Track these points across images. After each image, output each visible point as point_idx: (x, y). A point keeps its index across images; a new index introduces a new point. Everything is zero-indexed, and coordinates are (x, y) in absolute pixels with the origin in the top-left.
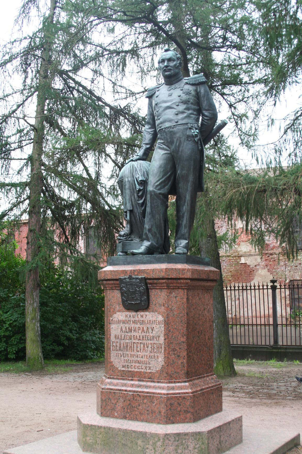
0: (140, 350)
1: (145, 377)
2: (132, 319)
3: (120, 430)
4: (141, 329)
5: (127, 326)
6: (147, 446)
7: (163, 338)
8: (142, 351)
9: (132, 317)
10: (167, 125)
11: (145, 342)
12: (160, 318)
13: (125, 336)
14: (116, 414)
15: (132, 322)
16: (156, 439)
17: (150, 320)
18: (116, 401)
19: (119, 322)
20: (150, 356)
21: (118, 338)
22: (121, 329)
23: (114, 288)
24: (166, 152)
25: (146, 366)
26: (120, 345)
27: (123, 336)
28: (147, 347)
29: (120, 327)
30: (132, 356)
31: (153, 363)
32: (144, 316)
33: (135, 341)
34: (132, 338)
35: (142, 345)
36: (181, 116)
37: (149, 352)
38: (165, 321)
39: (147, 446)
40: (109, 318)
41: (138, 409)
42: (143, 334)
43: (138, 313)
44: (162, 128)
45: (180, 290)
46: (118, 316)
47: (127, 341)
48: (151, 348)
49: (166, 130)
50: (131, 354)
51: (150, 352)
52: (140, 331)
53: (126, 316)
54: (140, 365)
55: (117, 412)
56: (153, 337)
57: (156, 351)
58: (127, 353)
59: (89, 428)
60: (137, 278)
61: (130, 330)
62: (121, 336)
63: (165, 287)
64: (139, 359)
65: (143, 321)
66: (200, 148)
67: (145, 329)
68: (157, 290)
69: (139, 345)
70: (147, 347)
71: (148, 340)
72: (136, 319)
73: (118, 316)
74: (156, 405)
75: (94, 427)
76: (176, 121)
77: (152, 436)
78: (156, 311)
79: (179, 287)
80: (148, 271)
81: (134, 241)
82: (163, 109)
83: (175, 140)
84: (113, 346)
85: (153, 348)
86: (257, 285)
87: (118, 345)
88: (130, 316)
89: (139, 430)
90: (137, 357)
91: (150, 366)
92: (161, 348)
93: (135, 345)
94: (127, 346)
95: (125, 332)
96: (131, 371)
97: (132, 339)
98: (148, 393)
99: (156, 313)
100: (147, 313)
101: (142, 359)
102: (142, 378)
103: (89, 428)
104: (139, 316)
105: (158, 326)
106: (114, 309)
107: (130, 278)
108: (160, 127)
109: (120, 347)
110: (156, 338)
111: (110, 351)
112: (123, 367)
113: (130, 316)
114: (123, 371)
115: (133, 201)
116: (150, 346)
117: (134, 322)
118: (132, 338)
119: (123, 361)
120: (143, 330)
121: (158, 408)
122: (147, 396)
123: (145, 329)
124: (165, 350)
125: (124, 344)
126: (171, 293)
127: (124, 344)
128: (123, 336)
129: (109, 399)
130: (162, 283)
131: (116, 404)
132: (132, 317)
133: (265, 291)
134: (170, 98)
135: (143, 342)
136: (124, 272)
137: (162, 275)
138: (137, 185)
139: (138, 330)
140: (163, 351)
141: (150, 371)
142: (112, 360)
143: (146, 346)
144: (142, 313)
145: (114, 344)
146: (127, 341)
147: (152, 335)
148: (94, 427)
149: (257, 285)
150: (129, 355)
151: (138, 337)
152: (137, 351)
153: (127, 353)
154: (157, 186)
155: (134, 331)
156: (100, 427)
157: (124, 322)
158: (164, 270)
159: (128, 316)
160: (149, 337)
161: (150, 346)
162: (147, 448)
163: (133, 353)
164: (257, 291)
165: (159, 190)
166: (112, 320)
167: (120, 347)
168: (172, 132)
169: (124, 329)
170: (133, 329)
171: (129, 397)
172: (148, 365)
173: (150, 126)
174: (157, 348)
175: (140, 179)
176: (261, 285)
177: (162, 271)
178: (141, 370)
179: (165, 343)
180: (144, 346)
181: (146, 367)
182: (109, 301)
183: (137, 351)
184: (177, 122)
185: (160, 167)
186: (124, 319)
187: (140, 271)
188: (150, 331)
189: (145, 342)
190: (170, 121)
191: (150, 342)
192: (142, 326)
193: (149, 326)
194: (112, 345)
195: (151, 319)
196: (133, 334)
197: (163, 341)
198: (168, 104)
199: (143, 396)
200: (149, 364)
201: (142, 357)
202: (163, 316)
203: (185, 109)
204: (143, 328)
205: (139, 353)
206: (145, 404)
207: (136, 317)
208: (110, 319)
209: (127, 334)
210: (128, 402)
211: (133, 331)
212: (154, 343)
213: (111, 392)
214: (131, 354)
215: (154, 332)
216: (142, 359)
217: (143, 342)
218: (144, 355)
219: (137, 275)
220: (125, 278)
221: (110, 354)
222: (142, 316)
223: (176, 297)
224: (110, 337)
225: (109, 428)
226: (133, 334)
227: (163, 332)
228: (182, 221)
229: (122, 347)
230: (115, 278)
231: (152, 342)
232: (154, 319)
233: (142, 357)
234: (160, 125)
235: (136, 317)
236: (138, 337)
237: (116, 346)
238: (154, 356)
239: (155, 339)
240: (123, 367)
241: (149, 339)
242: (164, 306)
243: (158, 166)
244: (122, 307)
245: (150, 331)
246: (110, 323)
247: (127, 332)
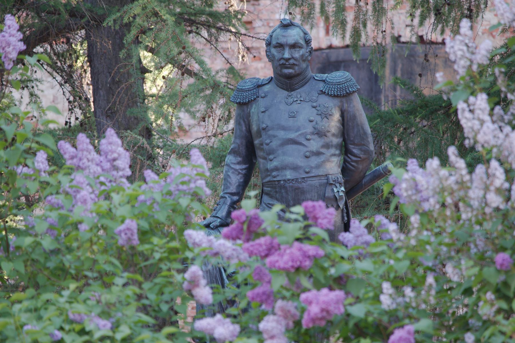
10: (289, 175)
44: (278, 178)
66: (346, 218)
76: (307, 170)
82: (279, 142)
168: (298, 188)
173: (239, 159)
184: (307, 173)
190: (295, 168)
198: (292, 135)
203: (323, 146)
234: (274, 173)
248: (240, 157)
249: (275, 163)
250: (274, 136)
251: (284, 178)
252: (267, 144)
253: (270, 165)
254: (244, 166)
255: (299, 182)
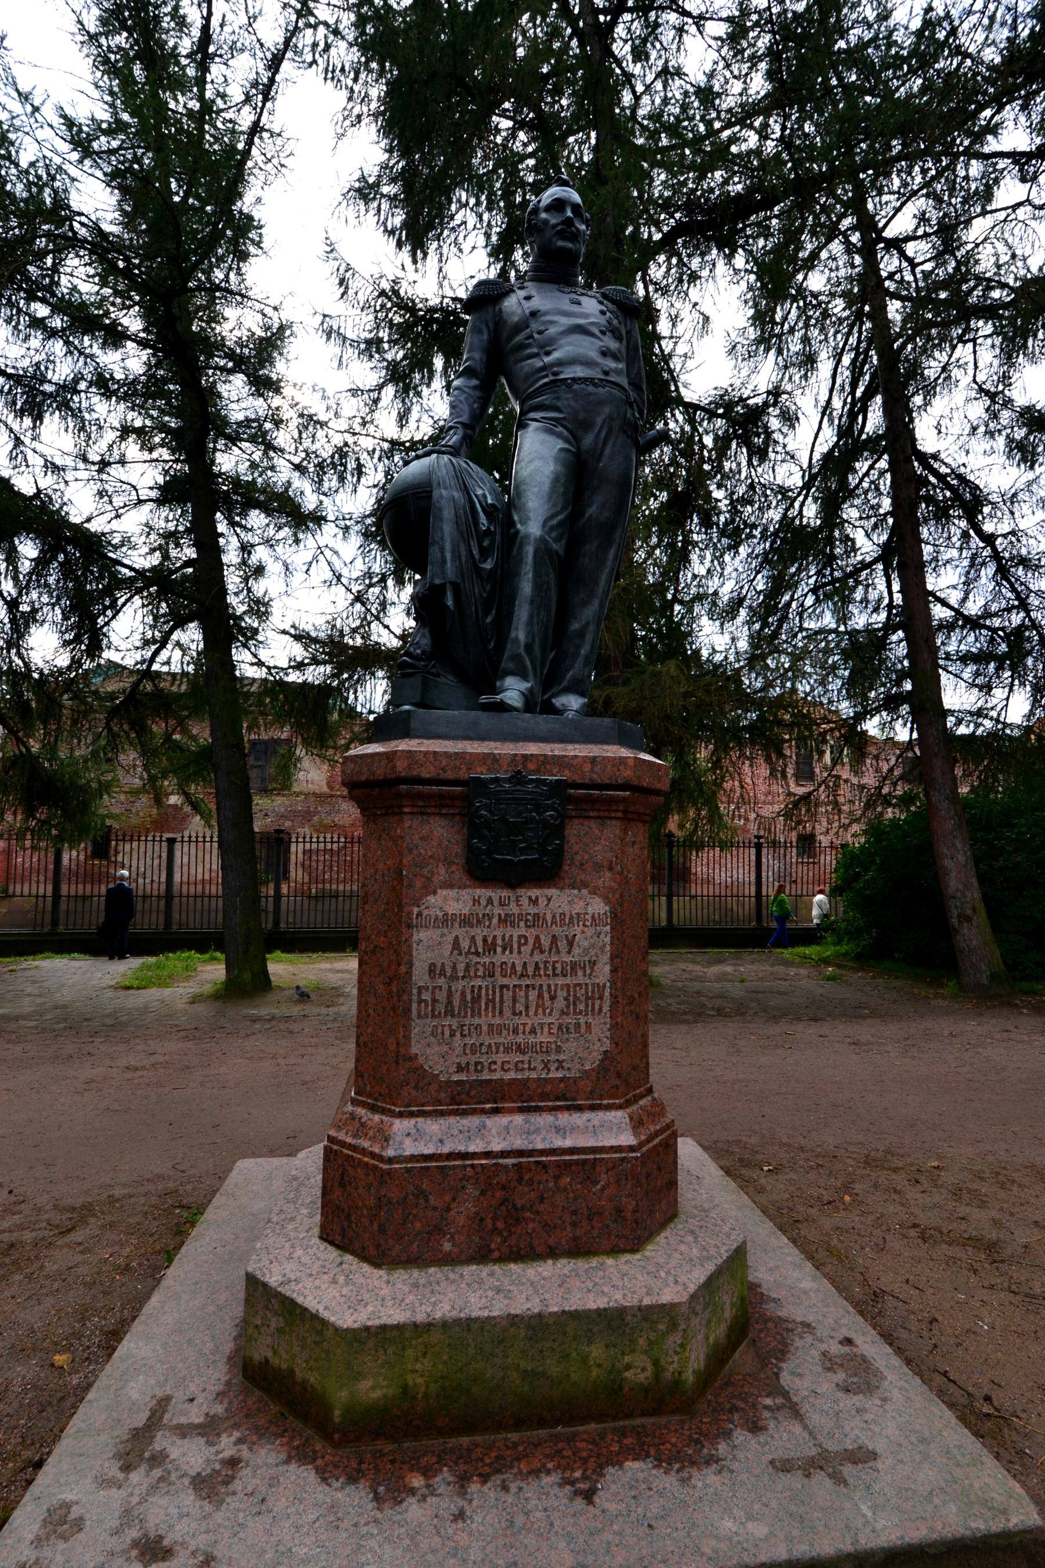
0: (527, 1008)
1: (543, 1097)
2: (497, 911)
3: (513, 1320)
4: (531, 941)
5: (479, 932)
6: (627, 1359)
7: (607, 968)
8: (531, 1013)
9: (496, 903)
10: (580, 372)
11: (544, 981)
12: (598, 907)
13: (468, 966)
14: (447, 1246)
15: (495, 921)
16: (662, 1327)
17: (563, 914)
18: (447, 1198)
19: (446, 920)
20: (560, 1027)
21: (443, 973)
22: (456, 944)
23: (437, 811)
24: (566, 446)
25: (546, 1058)
26: (450, 994)
27: (461, 967)
28: (553, 998)
29: (450, 938)
30: (499, 1029)
31: (571, 1047)
32: (542, 902)
33: (505, 981)
34: (498, 970)
35: (533, 995)
36: (612, 364)
37: (556, 1014)
38: (614, 916)
39: (627, 1359)
40: (406, 909)
41: (538, 1213)
42: (537, 957)
43: (521, 891)
44: (562, 376)
45: (640, 825)
46: (445, 899)
47: (478, 982)
48: (566, 999)
49: (576, 387)
50: (490, 1025)
51: (563, 1013)
52: (526, 949)
53: (476, 901)
54: (526, 1058)
55: (452, 1238)
56: (574, 966)
57: (582, 1007)
58: (477, 1021)
59: (371, 1344)
60: (543, 782)
61: (490, 947)
62: (454, 968)
63: (620, 814)
64: (520, 1039)
65: (536, 916)
67: (545, 942)
68: (586, 822)
69: (522, 994)
70: (553, 998)
71: (555, 975)
72: (513, 909)
73: (445, 899)
74: (603, 1189)
75: (395, 1333)
77: (645, 1319)
78: (584, 885)
79: (639, 814)
80: (575, 762)
81: (441, 680)
82: (562, 329)
83: (599, 420)
84: (420, 1002)
85: (571, 1002)
86: (194, 834)
87: (442, 996)
88: (490, 901)
89: (592, 1306)
90: (515, 1031)
91: (562, 1057)
92: (601, 998)
93: (508, 995)
94: (476, 1000)
95: (469, 953)
96: (490, 1081)
97: (497, 974)
98: (572, 1151)
99: (584, 891)
100: (553, 892)
101: (532, 1039)
102: (531, 1099)
103: (371, 1344)
104: (525, 902)
105: (590, 932)
106: (429, 879)
107: (518, 778)
108: (556, 374)
109: (450, 1003)
110: (584, 969)
111: (410, 1019)
112: (460, 1069)
113: (490, 901)
114: (460, 1083)
115: (464, 559)
116: (561, 994)
117: (503, 921)
118: (498, 970)
119: (459, 1050)
120: (538, 946)
121: (610, 1199)
122: (568, 1164)
123: (545, 942)
124: (614, 1004)
125: (463, 994)
126: (625, 831)
127: (463, 994)
128: (461, 967)
129: (421, 1194)
130: (611, 800)
131: (448, 1209)
132: (496, 903)
133: (208, 845)
134: (575, 308)
135: (538, 982)
136: (492, 760)
137: (627, 774)
138: (482, 515)
139: (520, 945)
140: (606, 1008)
141: (560, 1075)
142: (415, 1049)
143: (546, 996)
144: (534, 893)
145: (426, 996)
146: (478, 982)
147: (568, 959)
148: (395, 1333)
149: (194, 834)
150: (485, 1028)
151: (519, 969)
152: (514, 1014)
153: (477, 1021)
154: (552, 528)
155: (504, 949)
156: (417, 1329)
157: (466, 921)
158: (631, 763)
159: (483, 902)
160: (558, 966)
161: (561, 994)
162: (628, 1367)
163: (497, 1021)
164: (193, 845)
165: (556, 540)
166: (419, 914)
167: (450, 1003)
169: (465, 945)
170: (499, 942)
171: (503, 1177)
172: (553, 1057)
173: (474, 382)
174: (588, 998)
175: (490, 501)
176: (201, 835)
177: (626, 764)
178: (526, 1074)
179: (613, 983)
180: (540, 996)
181: (546, 1065)
182: (410, 851)
183: (514, 1014)
184: (606, 373)
185: (556, 480)
186: (466, 911)
187: (545, 761)
188: (562, 945)
189: (544, 981)
190: (588, 363)
191: (560, 981)
192: (531, 934)
193: (557, 930)
194: (415, 998)
195: (566, 909)
196: (499, 958)
197: (608, 976)
198: (581, 321)
199: (558, 1165)
200: (559, 1051)
201: (533, 1031)
202: (607, 900)
204: (537, 938)
205: (524, 1019)
206: (565, 1189)
207: (513, 904)
208: (410, 913)
209: (476, 959)
210: (499, 1194)
211: (499, 950)
212: (576, 985)
213: (428, 1168)
214: (490, 1025)
215: (576, 951)
216: (532, 1039)
217: (538, 982)
218: (542, 1025)
219: (537, 771)
220: (496, 780)
221: (407, 1028)
222: (534, 902)
223: (634, 843)
224: (409, 973)
225: (469, 1324)
226: (499, 958)
227: (608, 948)
228: (578, 647)
229: (456, 1002)
230: (450, 775)
231: (568, 980)
232: (578, 907)
233: (533, 1031)
235: (513, 904)
236: (519, 969)
237: (435, 1001)
238: (578, 1025)
239: (580, 973)
240: (460, 1069)
241: (558, 971)
242: (610, 869)
243: (552, 476)
244: (459, 875)
245: (562, 945)
246: (409, 926)
247: (477, 954)
248: (477, 378)
249: (556, 355)
250: (552, 322)
251: (571, 376)
252: (540, 333)
253: (547, 359)
254: (478, 393)
255: (596, 385)
